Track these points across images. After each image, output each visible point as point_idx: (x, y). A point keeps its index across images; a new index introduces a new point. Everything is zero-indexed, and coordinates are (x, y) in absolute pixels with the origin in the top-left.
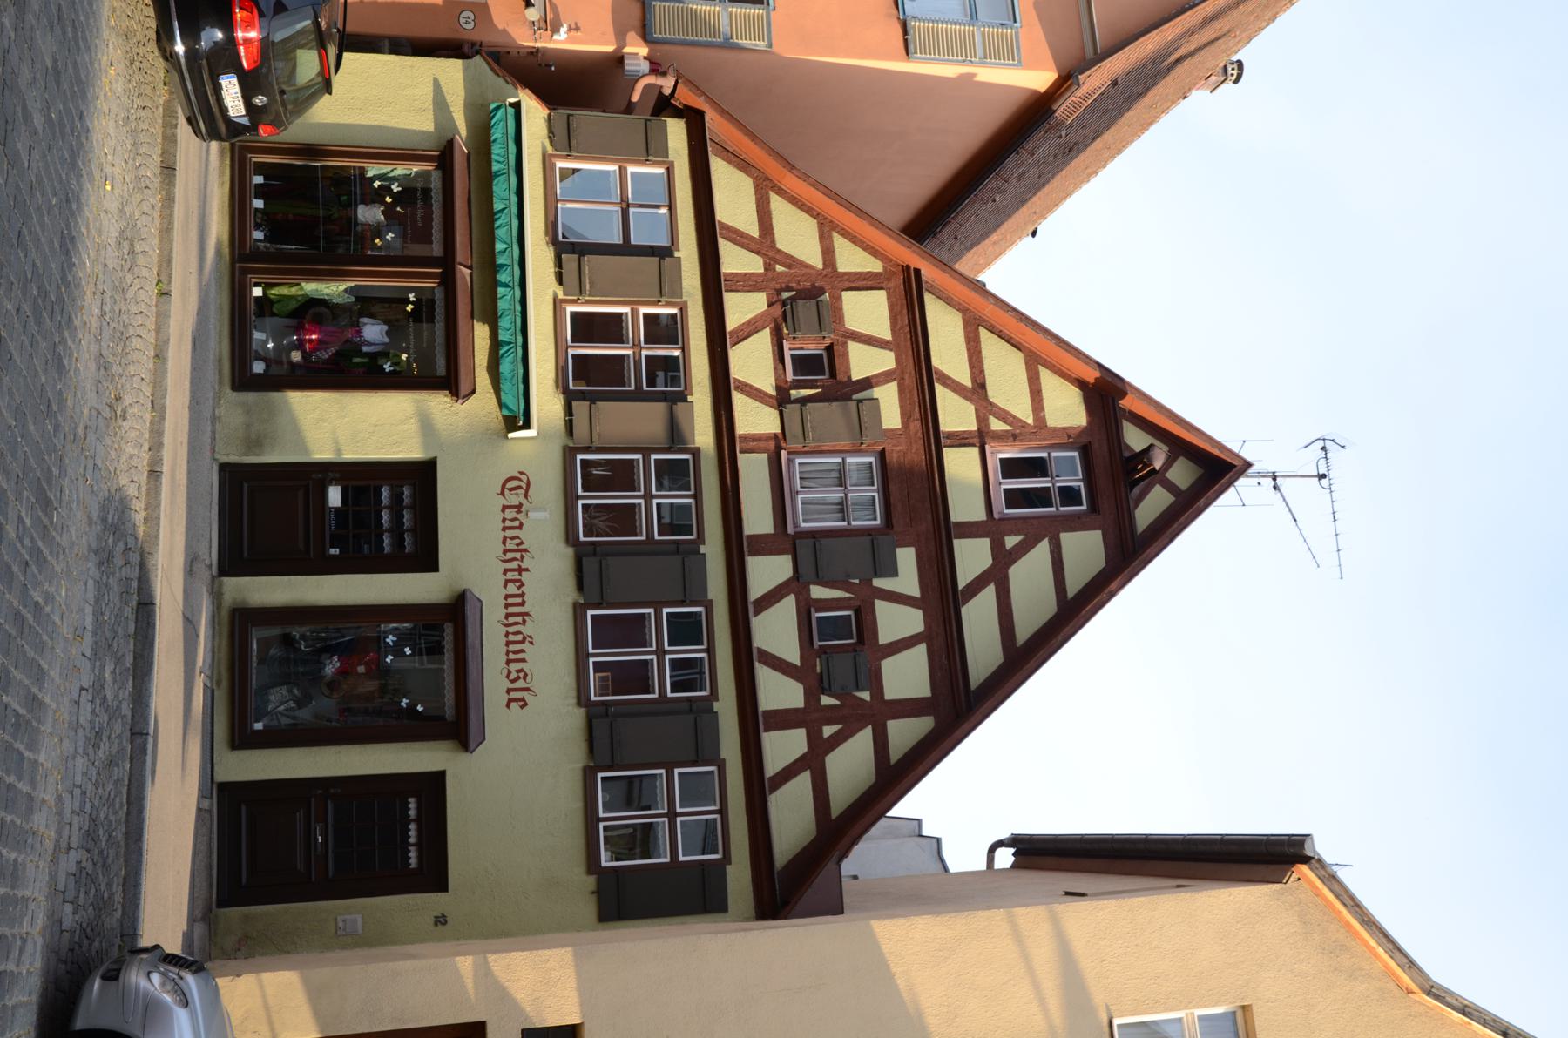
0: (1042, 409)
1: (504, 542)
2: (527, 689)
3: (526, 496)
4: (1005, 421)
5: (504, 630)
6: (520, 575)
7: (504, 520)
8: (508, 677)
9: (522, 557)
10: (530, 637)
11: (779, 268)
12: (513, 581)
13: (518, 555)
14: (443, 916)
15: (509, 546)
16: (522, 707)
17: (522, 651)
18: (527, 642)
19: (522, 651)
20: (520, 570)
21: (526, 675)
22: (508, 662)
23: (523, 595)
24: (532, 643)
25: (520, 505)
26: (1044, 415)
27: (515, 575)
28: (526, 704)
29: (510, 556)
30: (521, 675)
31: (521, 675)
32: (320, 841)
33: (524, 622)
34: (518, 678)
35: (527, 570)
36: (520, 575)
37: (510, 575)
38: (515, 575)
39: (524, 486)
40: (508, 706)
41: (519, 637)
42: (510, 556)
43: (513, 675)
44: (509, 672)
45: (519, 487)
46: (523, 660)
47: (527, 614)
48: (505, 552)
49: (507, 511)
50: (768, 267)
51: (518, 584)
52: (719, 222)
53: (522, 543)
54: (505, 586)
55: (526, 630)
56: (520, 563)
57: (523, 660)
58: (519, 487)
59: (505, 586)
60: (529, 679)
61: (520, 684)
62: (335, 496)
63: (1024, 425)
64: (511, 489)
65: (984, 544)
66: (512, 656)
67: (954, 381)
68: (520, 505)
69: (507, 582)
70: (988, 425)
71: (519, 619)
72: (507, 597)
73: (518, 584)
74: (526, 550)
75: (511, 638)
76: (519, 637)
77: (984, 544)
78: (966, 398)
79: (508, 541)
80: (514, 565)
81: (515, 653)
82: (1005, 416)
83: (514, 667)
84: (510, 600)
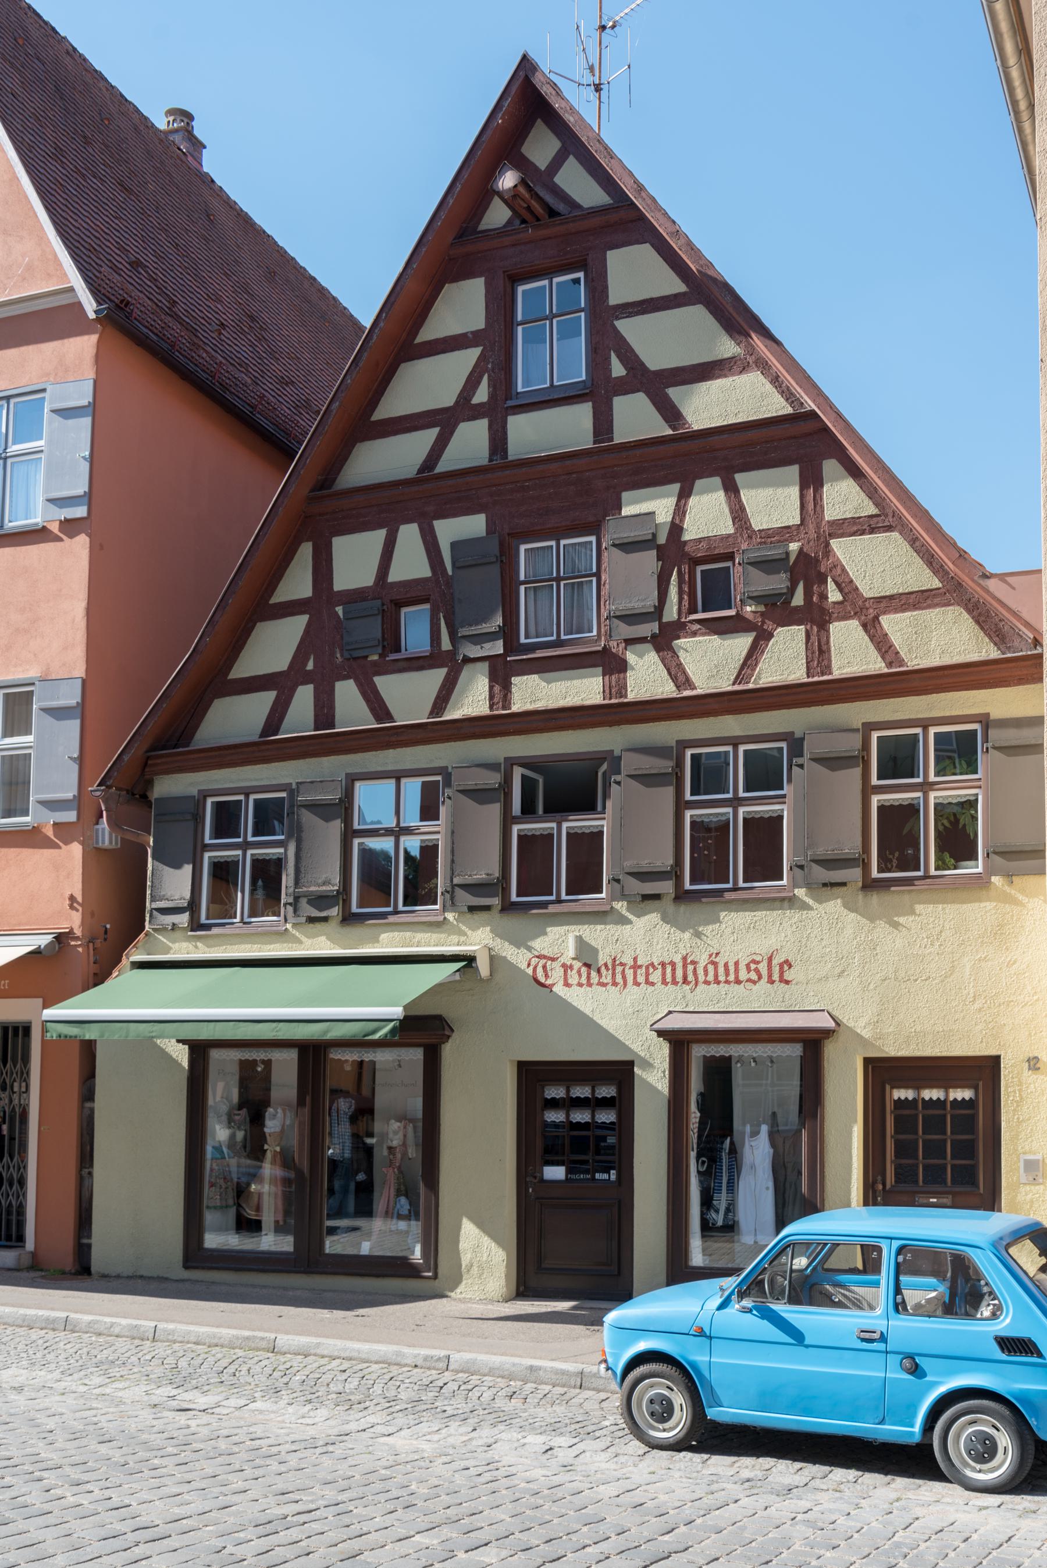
0: (464, 335)
1: (604, 985)
2: (770, 959)
3: (553, 959)
5: (701, 987)
6: (640, 967)
7: (580, 985)
8: (754, 982)
9: (621, 964)
10: (711, 956)
11: (310, 666)
12: (647, 975)
13: (619, 969)
14: (1028, 1060)
15: (609, 979)
16: (790, 966)
17: (726, 965)
18: (717, 960)
19: (726, 965)
20: (636, 967)
21: (754, 962)
22: (738, 982)
23: (663, 965)
24: (717, 954)
25: (564, 965)
26: (472, 332)
27: (641, 972)
28: (787, 962)
29: (619, 979)
30: (753, 966)
31: (753, 966)
32: (935, 1200)
33: (693, 962)
34: (757, 971)
35: (635, 959)
36: (640, 967)
37: (641, 979)
38: (641, 972)
39: (544, 961)
40: (787, 982)
41: (711, 968)
42: (619, 979)
43: (754, 976)
44: (749, 980)
45: (544, 967)
46: (737, 964)
47: (685, 959)
48: (615, 984)
49: (570, 981)
51: (651, 970)
52: (261, 736)
53: (606, 965)
54: (653, 984)
55: (703, 961)
56: (628, 967)
57: (737, 964)
58: (544, 967)
59: (653, 984)
60: (758, 958)
61: (763, 968)
62: (555, 1173)
63: (482, 358)
64: (547, 976)
65: (620, 404)
66: (732, 978)
67: (432, 449)
68: (564, 965)
69: (647, 982)
70: (481, 405)
71: (690, 968)
72: (664, 982)
73: (651, 970)
74: (614, 960)
75: (711, 977)
76: (711, 968)
77: (620, 404)
78: (452, 433)
79: (604, 980)
80: (629, 973)
81: (727, 974)
82: (472, 383)
83: (743, 975)
84: (669, 978)
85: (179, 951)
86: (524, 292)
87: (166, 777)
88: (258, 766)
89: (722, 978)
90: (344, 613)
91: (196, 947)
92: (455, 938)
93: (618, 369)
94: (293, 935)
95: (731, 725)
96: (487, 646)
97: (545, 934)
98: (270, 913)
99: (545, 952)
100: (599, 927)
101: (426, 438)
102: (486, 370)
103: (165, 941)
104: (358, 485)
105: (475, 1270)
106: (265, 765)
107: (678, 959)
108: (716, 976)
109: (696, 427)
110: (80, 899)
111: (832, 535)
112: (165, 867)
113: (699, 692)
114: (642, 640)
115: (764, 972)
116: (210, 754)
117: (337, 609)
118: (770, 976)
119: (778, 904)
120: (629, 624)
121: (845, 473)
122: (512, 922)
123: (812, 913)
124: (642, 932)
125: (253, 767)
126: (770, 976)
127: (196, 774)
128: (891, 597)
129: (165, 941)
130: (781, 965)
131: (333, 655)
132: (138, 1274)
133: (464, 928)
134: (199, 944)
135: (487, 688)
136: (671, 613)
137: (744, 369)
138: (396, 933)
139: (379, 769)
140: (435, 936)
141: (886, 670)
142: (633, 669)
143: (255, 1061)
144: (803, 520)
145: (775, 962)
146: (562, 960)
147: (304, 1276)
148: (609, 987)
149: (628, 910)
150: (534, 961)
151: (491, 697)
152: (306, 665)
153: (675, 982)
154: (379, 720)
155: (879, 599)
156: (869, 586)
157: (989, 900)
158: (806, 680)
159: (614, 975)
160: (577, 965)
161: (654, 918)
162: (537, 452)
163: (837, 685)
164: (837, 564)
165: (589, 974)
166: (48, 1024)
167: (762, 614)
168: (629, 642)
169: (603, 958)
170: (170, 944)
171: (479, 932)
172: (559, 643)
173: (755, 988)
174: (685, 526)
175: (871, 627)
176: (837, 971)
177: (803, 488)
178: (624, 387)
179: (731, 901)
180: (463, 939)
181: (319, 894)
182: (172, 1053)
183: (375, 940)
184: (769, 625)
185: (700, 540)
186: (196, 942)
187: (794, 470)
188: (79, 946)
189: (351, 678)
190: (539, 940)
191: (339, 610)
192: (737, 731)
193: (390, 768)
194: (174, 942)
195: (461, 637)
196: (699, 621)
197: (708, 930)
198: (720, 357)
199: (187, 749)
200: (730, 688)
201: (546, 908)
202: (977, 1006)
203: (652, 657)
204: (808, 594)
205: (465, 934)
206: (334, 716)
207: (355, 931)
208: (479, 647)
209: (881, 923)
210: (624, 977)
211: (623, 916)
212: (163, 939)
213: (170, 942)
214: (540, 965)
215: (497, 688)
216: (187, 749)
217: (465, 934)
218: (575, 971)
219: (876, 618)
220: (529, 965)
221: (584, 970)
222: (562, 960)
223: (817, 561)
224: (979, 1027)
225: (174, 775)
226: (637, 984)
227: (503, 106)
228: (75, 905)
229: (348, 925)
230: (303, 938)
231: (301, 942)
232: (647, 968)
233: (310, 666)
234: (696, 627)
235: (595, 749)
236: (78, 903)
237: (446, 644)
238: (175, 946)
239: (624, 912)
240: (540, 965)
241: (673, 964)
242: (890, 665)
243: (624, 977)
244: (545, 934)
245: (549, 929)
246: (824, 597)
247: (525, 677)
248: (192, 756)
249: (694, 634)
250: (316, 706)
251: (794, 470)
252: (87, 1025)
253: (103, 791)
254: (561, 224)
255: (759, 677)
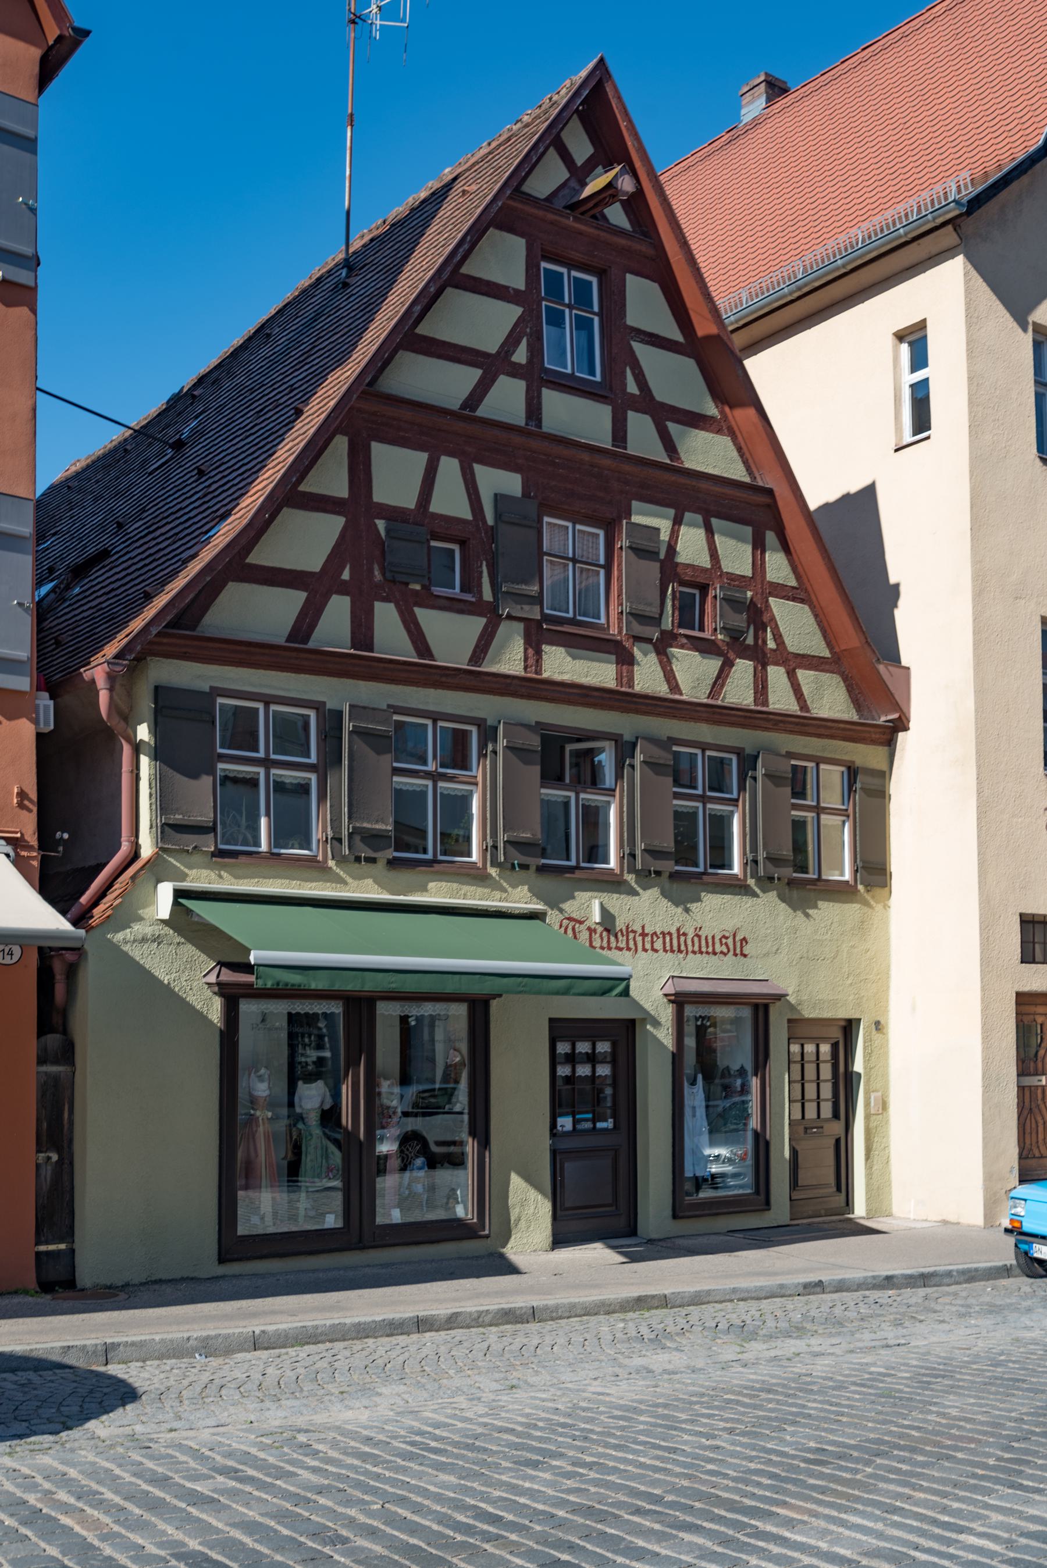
2: (734, 935)
3: (581, 923)
4: (518, 343)
5: (690, 955)
6: (647, 935)
8: (725, 954)
11: (346, 575)
12: (652, 942)
13: (631, 936)
15: (623, 945)
17: (706, 937)
21: (724, 937)
22: (715, 953)
23: (663, 933)
25: (589, 929)
26: (514, 289)
27: (648, 939)
28: (744, 939)
29: (631, 944)
30: (724, 941)
31: (724, 941)
33: (685, 934)
34: (726, 944)
35: (643, 927)
36: (647, 935)
37: (648, 946)
38: (648, 939)
39: (572, 924)
40: (745, 956)
41: (696, 939)
42: (631, 944)
44: (722, 952)
45: (573, 929)
46: (713, 937)
47: (678, 930)
48: (629, 949)
49: (594, 944)
50: (343, 589)
53: (621, 930)
57: (713, 937)
58: (573, 929)
59: (656, 951)
60: (727, 934)
61: (730, 941)
66: (710, 949)
68: (589, 929)
71: (682, 939)
75: (696, 948)
81: (707, 947)
82: (511, 342)
85: (198, 879)
86: (590, 283)
87: (164, 660)
88: (285, 674)
89: (704, 949)
90: (388, 531)
91: (220, 877)
92: (497, 894)
93: (520, 355)
94: (337, 874)
95: (705, 732)
96: (526, 607)
97: (573, 898)
98: (297, 845)
99: (574, 915)
100: (615, 896)
101: (468, 377)
102: (525, 334)
103: (178, 865)
104: (407, 396)
105: (523, 1224)
106: (293, 675)
107: (674, 931)
108: (700, 947)
109: (688, 465)
110: (34, 796)
111: (771, 594)
112: (175, 773)
113: (684, 698)
114: (649, 641)
115: (731, 947)
116: (238, 648)
117: (377, 521)
118: (735, 950)
119: (737, 889)
120: (641, 624)
121: (780, 547)
122: (548, 883)
123: (759, 900)
124: (647, 904)
125: (279, 673)
126: (735, 950)
127: (205, 666)
128: (803, 656)
129: (178, 865)
130: (741, 941)
131: (371, 571)
132: (153, 1279)
133: (505, 884)
134: (224, 874)
135: (522, 649)
136: (667, 623)
137: (719, 432)
138: (444, 884)
139: (421, 707)
140: (480, 890)
141: (799, 713)
142: (639, 664)
143: (316, 1015)
144: (753, 574)
145: (738, 938)
146: (587, 924)
147: (358, 1252)
148: (624, 951)
149: (636, 882)
150: (565, 922)
151: (526, 659)
152: (341, 573)
153: (672, 951)
154: (420, 655)
155: (797, 656)
156: (792, 644)
157: (856, 902)
158: (753, 707)
159: (628, 940)
160: (600, 929)
161: (655, 892)
162: (587, 438)
163: (693, 708)
164: (773, 619)
165: (609, 939)
166: (261, 968)
167: (728, 644)
168: (637, 639)
169: (620, 924)
170: (186, 870)
171: (519, 889)
172: (573, 622)
173: (726, 959)
174: (678, 549)
175: (791, 675)
176: (774, 949)
177: (754, 549)
178: (515, 372)
179: (707, 884)
180: (504, 895)
181: (375, 832)
182: (195, 1004)
183: (424, 889)
184: (731, 655)
185: (688, 566)
186: (219, 871)
187: (672, 512)
188: (33, 858)
189: (347, 594)
190: (569, 903)
191: (381, 525)
192: (709, 739)
193: (431, 708)
194: (190, 868)
195: (507, 593)
196: (687, 636)
197: (694, 906)
198: (703, 412)
199: (302, 646)
200: (705, 701)
201: (573, 873)
202: (849, 982)
203: (653, 658)
204: (756, 638)
205: (506, 891)
206: (372, 638)
207: (406, 876)
208: (519, 607)
209: (799, 913)
210: (635, 944)
211: (632, 887)
212: (175, 863)
213: (186, 867)
214: (570, 927)
215: (531, 651)
216: (302, 646)
217: (506, 891)
218: (598, 935)
219: (794, 670)
220: (561, 926)
221: (605, 934)
222: (587, 924)
223: (762, 613)
224: (851, 998)
225: (175, 661)
226: (645, 950)
227: (581, 95)
228: (26, 802)
229: (394, 869)
230: (349, 880)
231: (345, 883)
232: (652, 936)
233: (346, 575)
234: (684, 641)
235: (609, 730)
236: (31, 801)
237: (487, 595)
238: (193, 873)
239: (633, 884)
240: (570, 927)
241: (670, 934)
242: (801, 709)
243: (635, 944)
244: (573, 898)
245: (576, 894)
246: (765, 642)
247: (554, 648)
248: (211, 645)
249: (682, 647)
250: (352, 622)
251: (672, 512)
252: (311, 972)
253: (125, 666)
254: (596, 228)
255: (724, 697)
